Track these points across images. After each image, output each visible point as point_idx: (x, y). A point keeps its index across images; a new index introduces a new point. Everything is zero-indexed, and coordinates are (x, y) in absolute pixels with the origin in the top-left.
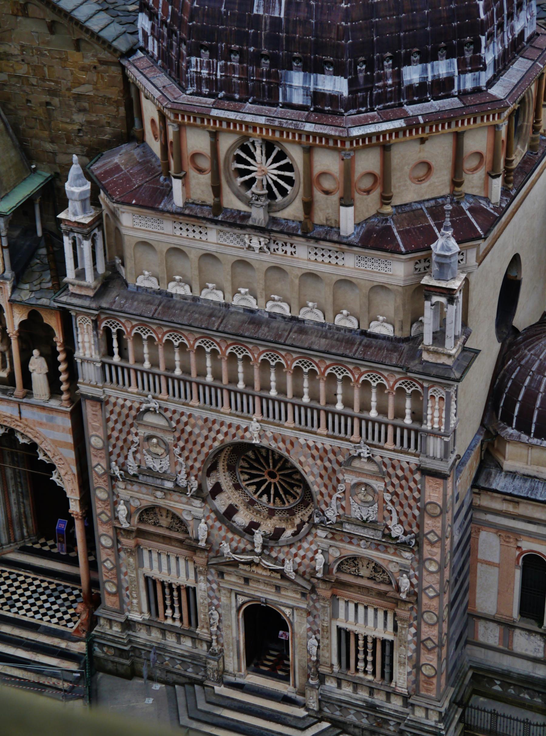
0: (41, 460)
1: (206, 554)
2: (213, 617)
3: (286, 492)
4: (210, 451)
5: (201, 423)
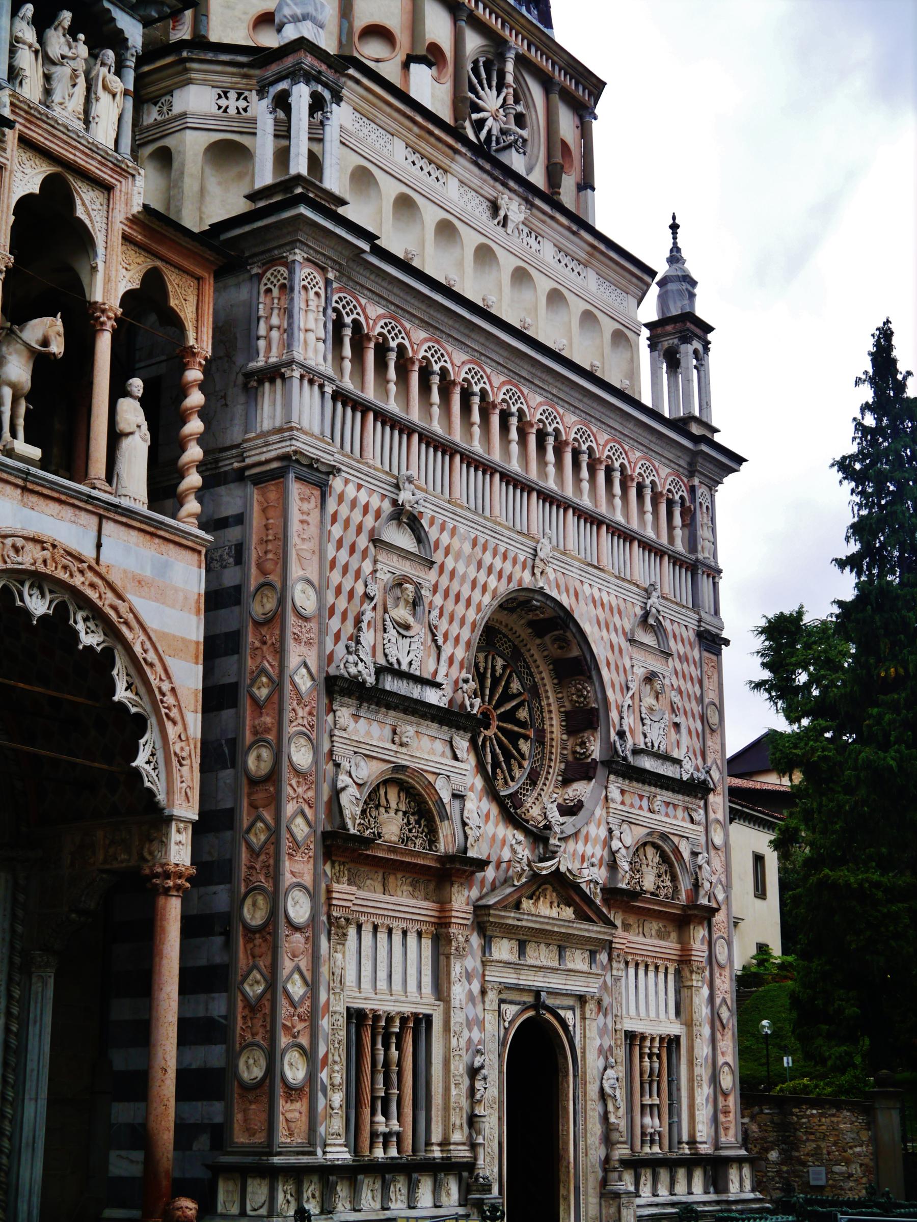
0: (120, 703)
1: (466, 893)
2: (484, 1072)
3: (508, 756)
4: (478, 618)
5: (467, 548)
